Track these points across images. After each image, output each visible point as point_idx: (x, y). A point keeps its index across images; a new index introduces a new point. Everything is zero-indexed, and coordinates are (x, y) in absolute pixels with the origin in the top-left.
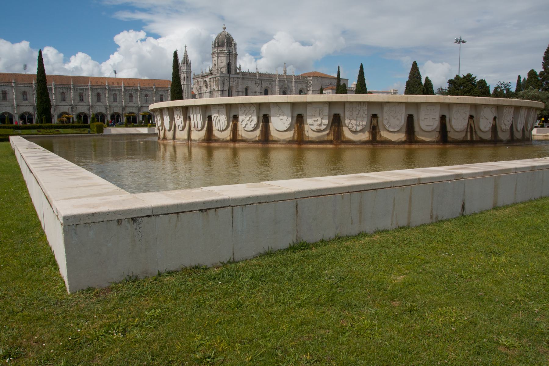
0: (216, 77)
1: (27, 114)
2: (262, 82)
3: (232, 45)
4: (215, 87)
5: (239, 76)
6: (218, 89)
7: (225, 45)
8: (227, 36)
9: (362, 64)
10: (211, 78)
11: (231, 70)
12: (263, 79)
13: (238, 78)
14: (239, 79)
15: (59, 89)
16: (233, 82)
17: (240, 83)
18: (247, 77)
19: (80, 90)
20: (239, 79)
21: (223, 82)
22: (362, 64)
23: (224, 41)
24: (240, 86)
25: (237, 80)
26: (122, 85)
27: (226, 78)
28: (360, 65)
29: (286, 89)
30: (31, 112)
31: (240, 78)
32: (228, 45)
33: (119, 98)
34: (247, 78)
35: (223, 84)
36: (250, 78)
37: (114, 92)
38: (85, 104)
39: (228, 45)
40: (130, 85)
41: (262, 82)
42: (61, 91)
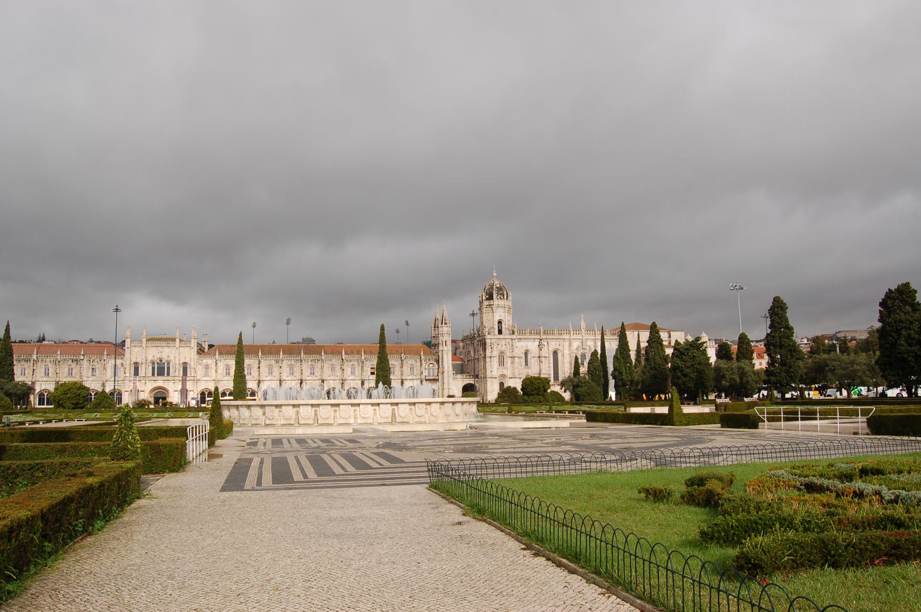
0: (483, 340)
1: (249, 391)
2: (548, 343)
3: (504, 297)
4: (481, 352)
5: (514, 337)
6: (485, 355)
7: (495, 296)
8: (498, 286)
9: (623, 322)
10: (478, 341)
11: (503, 330)
12: (549, 339)
13: (512, 339)
14: (514, 341)
15: (288, 361)
16: (505, 345)
17: (514, 347)
18: (527, 337)
19: (311, 361)
20: (514, 341)
21: (491, 345)
22: (623, 322)
23: (492, 292)
24: (516, 350)
25: (511, 343)
26: (363, 354)
27: (496, 340)
28: (621, 324)
29: (585, 351)
30: (254, 389)
31: (515, 339)
32: (498, 297)
33: (358, 370)
34: (526, 339)
35: (492, 348)
36: (530, 339)
37: (351, 363)
38: (316, 378)
39: (498, 297)
40: (373, 353)
41: (548, 343)
42: (290, 363)
